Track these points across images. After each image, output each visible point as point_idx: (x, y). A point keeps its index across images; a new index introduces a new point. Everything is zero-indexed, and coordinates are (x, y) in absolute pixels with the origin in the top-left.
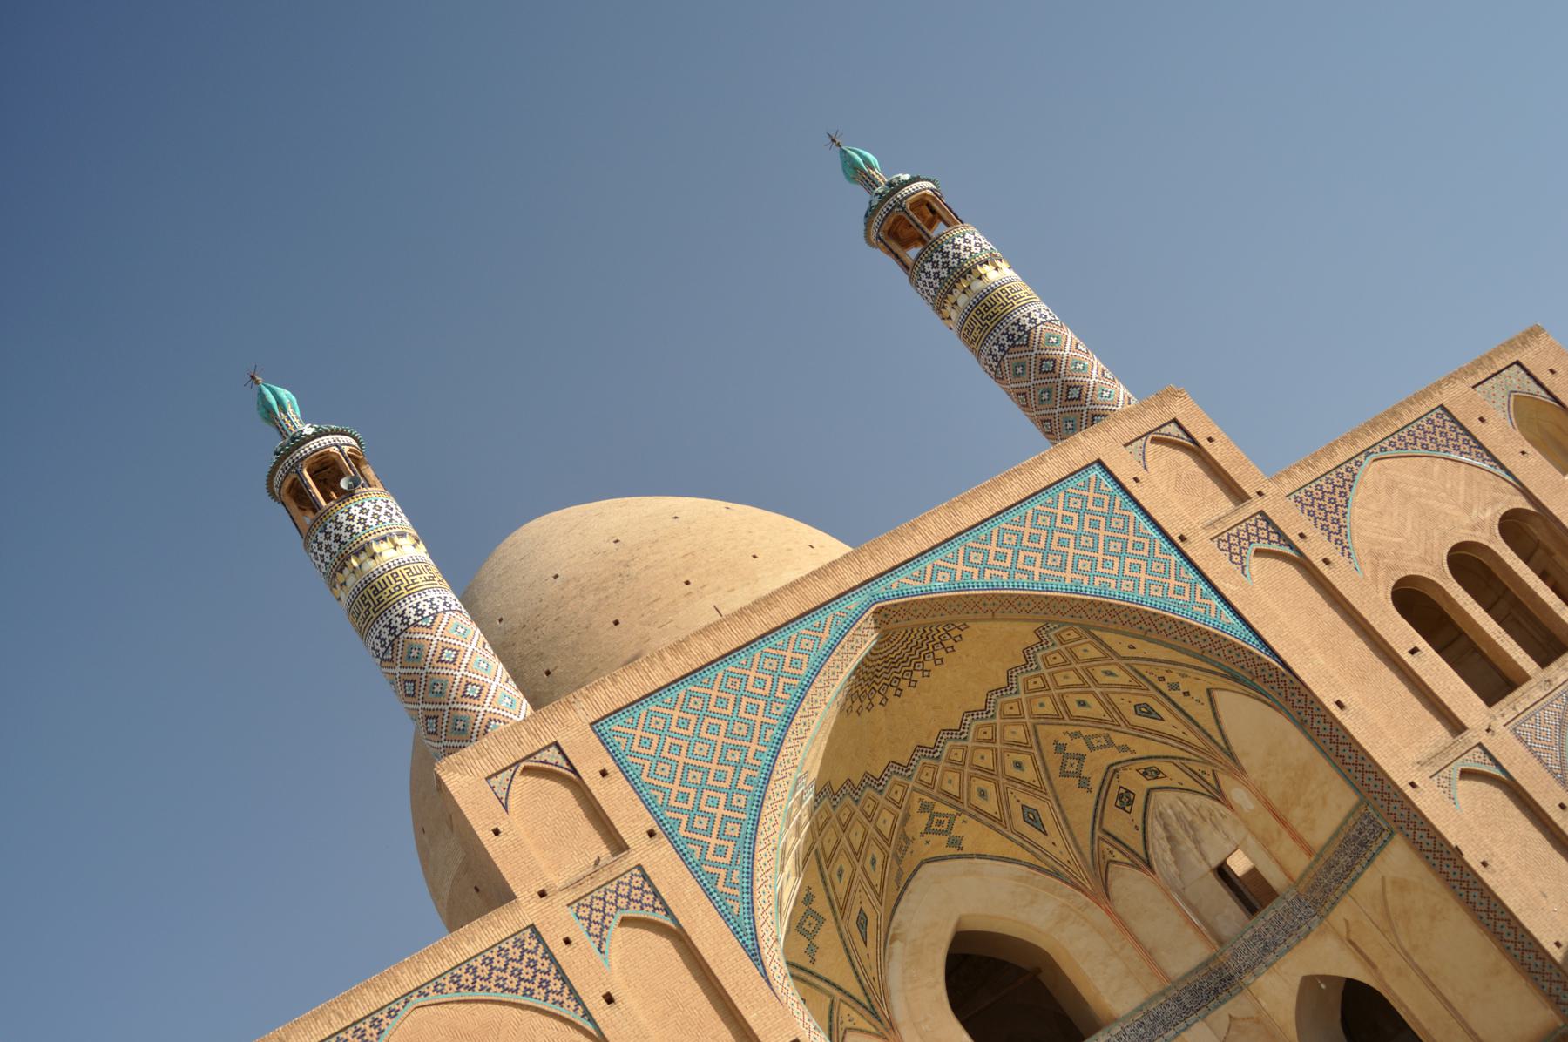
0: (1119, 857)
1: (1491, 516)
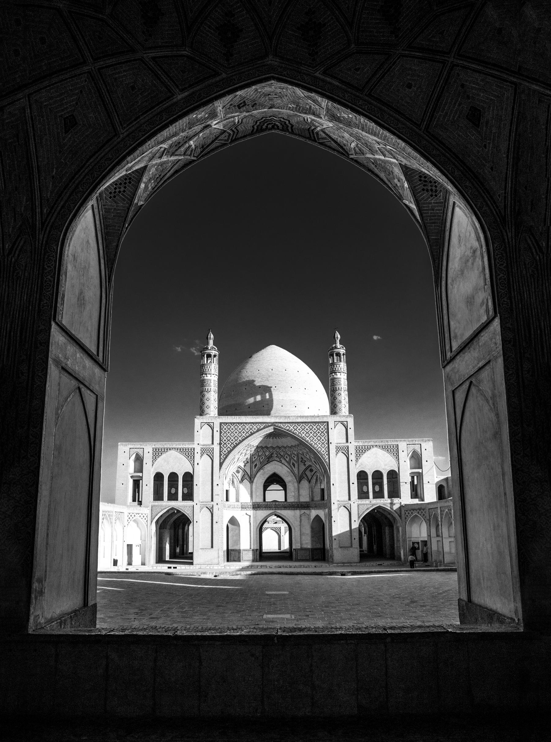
1: (389, 469)
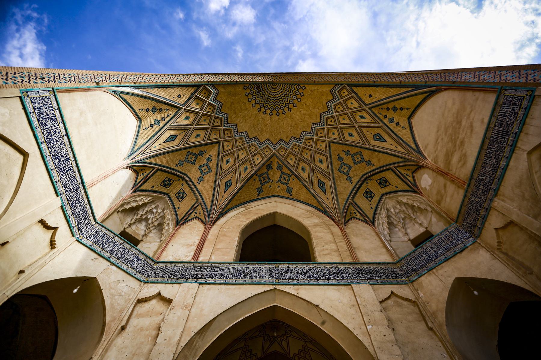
0: (358, 216)
